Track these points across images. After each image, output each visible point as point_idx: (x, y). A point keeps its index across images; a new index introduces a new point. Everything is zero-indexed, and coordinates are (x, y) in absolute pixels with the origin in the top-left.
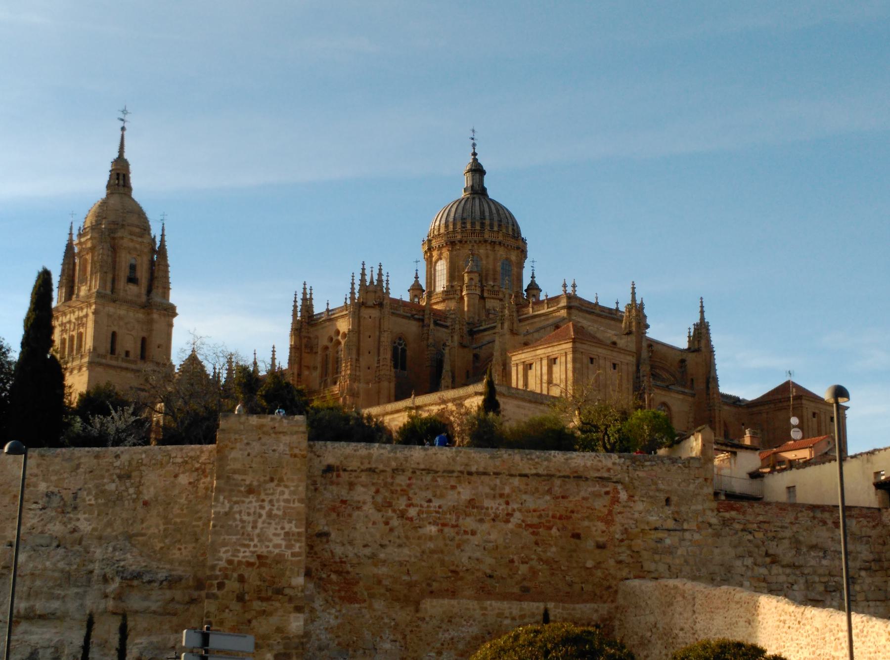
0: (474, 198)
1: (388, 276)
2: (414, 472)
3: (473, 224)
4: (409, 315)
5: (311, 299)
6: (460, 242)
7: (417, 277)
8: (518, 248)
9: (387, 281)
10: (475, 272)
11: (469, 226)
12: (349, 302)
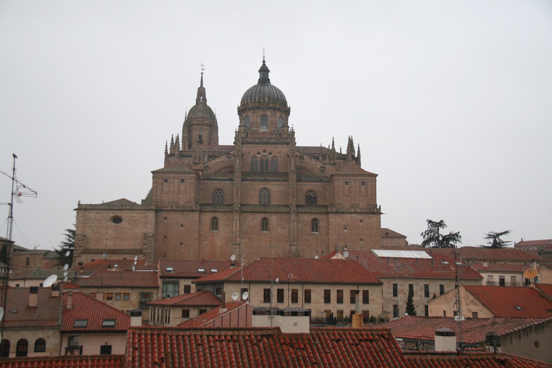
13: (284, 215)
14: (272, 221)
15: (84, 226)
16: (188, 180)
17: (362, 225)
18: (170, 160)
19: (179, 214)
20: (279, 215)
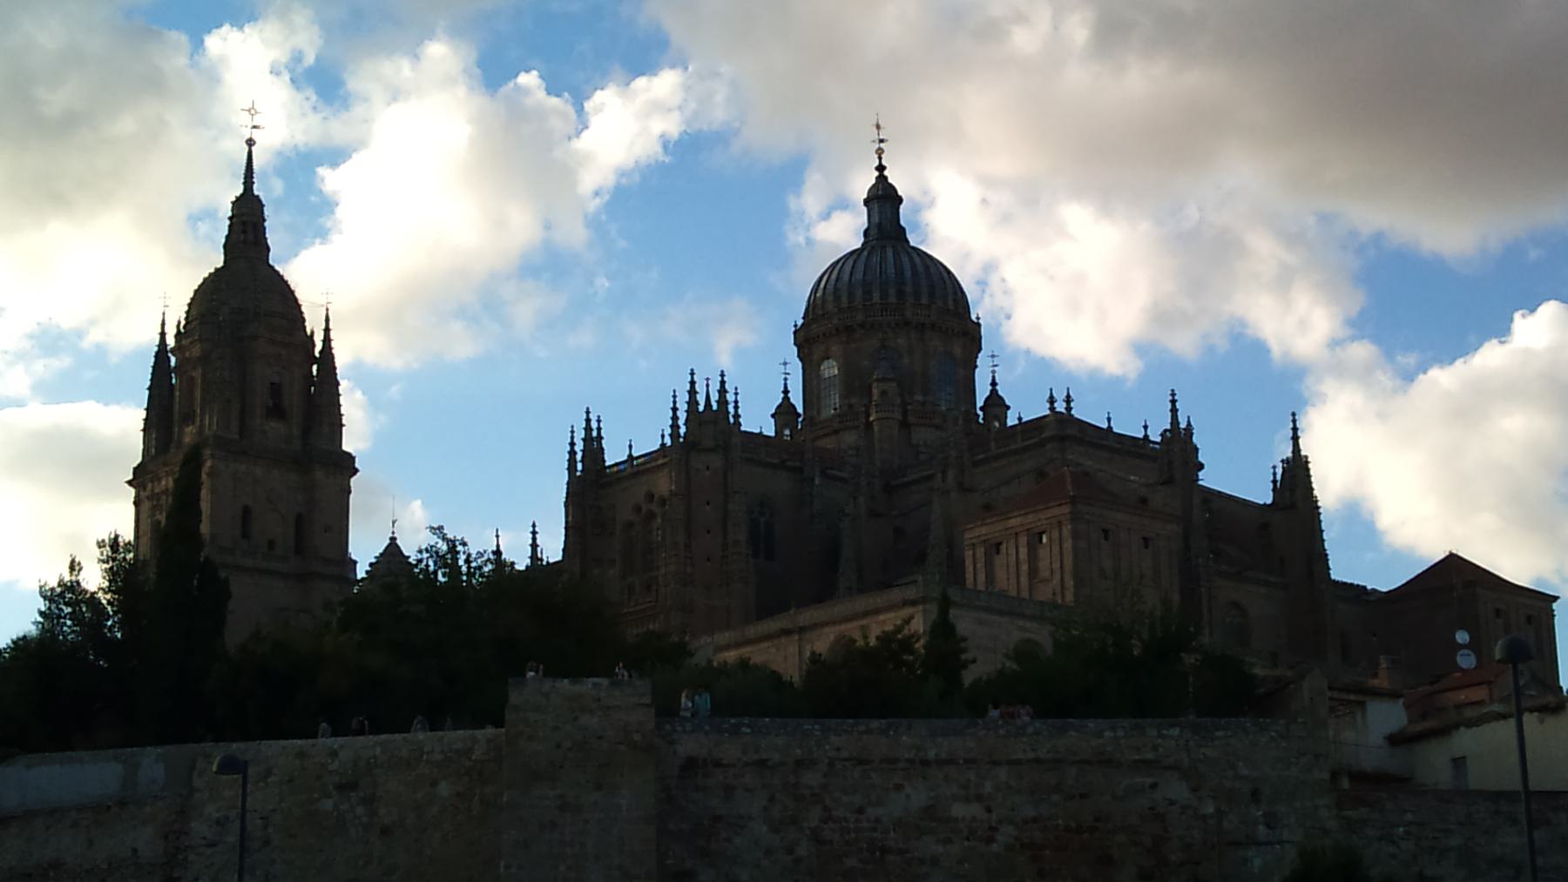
0: (883, 248)
1: (736, 394)
2: (831, 764)
3: (884, 295)
4: (776, 461)
5: (600, 438)
6: (862, 326)
7: (786, 392)
8: (965, 334)
9: (736, 402)
10: (890, 380)
11: (876, 297)
12: (668, 441)
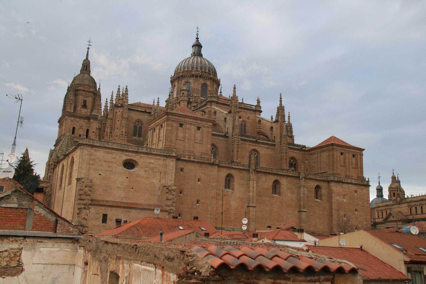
4: (144, 110)
6: (182, 76)
13: (293, 179)
14: (283, 184)
15: (89, 169)
16: (204, 129)
17: (357, 196)
18: (115, 111)
19: (197, 166)
20: (289, 179)
